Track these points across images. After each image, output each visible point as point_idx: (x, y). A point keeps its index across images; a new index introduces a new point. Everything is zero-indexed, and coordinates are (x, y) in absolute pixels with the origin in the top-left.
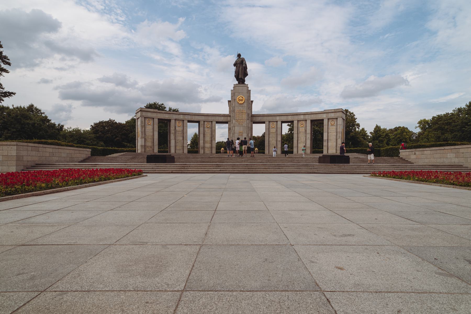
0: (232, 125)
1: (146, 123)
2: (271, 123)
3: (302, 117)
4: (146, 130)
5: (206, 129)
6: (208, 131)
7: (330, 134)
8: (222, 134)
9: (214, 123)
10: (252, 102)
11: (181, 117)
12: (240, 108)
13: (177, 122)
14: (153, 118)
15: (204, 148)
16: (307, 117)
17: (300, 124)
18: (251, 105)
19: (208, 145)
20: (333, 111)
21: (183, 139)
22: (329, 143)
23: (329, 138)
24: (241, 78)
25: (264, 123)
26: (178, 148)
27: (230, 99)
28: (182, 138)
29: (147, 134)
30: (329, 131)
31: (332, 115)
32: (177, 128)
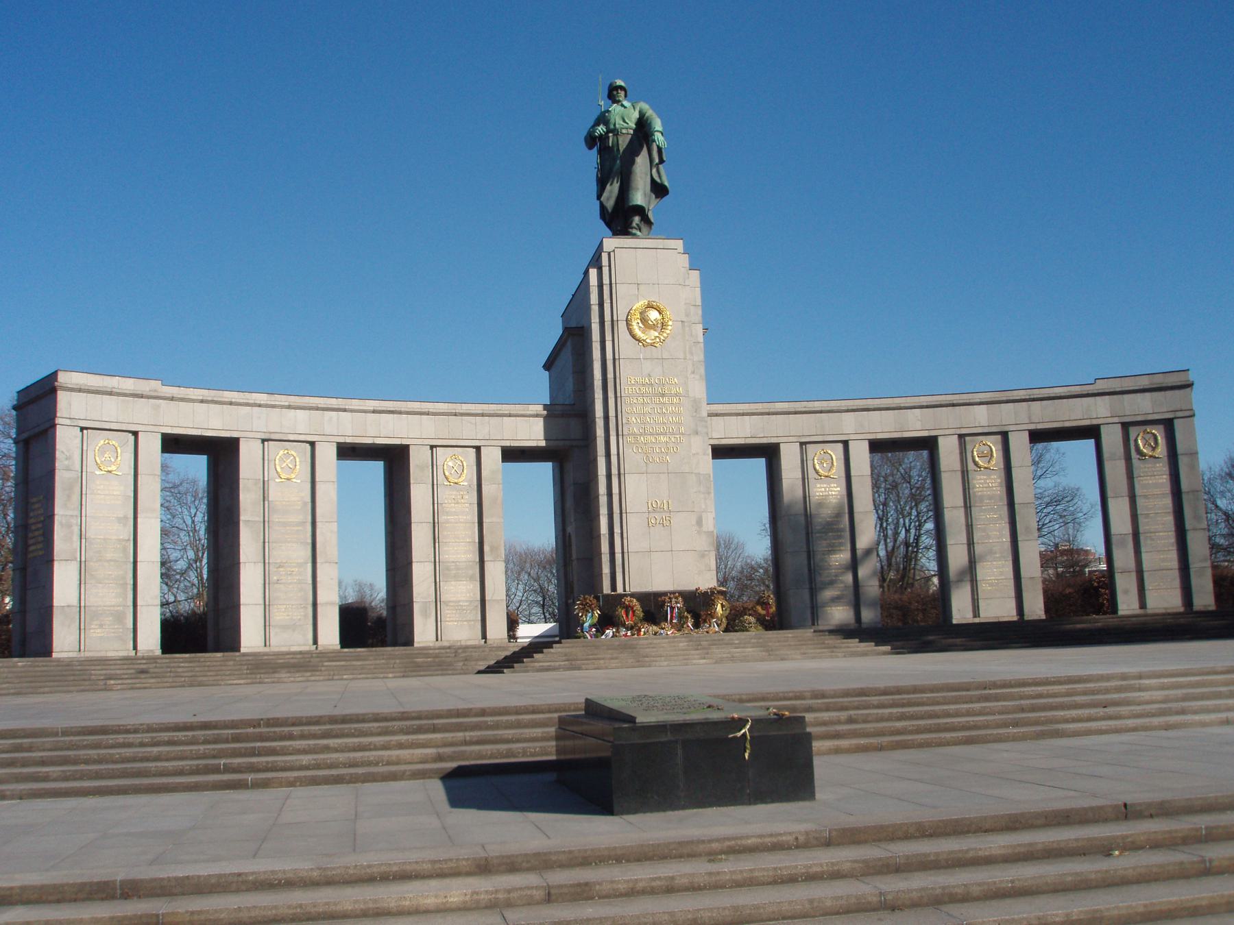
1: (90, 466)
3: (980, 417)
4: (89, 509)
5: (445, 495)
7: (1140, 502)
12: (647, 366)
13: (278, 453)
14: (135, 434)
16: (1007, 416)
19: (461, 591)
20: (1145, 382)
22: (1145, 557)
23: (1142, 528)
24: (640, 211)
26: (278, 616)
29: (93, 531)
30: (1138, 491)
31: (1144, 406)
32: (273, 494)
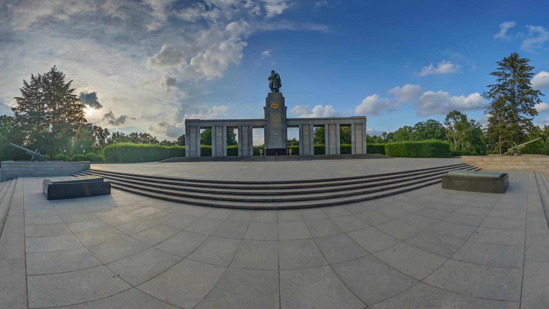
0: (267, 128)
2: (304, 127)
3: (332, 121)
6: (245, 135)
8: (258, 138)
9: (251, 127)
10: (286, 108)
11: (221, 124)
13: (217, 128)
15: (242, 150)
16: (336, 121)
17: (330, 128)
18: (286, 110)
21: (223, 143)
24: (276, 89)
25: (297, 126)
26: (218, 151)
27: (265, 106)
28: (221, 143)
